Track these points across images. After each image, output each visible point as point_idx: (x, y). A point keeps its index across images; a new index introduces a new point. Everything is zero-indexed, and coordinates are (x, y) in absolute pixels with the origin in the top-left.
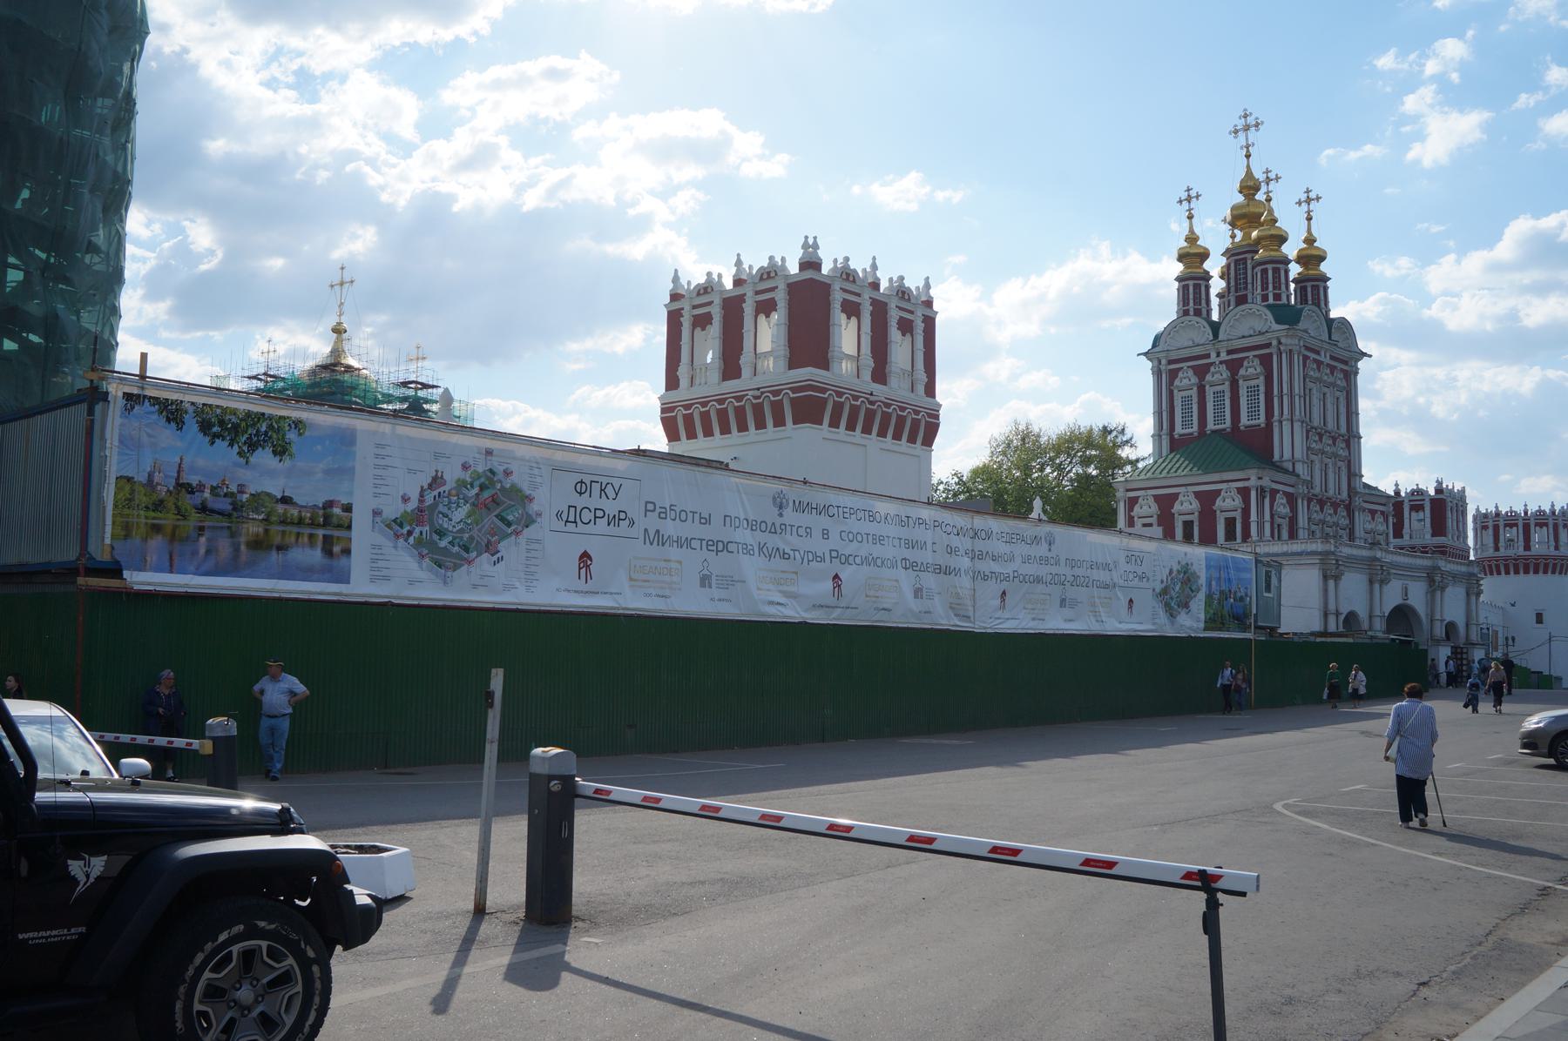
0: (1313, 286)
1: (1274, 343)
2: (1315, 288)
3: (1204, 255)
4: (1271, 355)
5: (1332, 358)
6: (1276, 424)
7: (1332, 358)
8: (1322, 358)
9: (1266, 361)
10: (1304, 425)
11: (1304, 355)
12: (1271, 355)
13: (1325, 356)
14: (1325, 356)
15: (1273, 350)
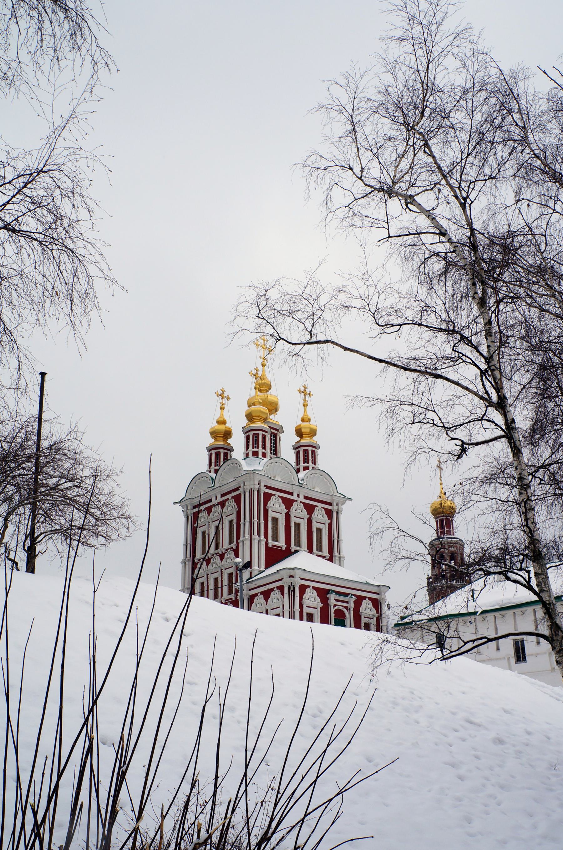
0: (304, 450)
1: (242, 485)
2: (306, 452)
3: (227, 434)
4: (240, 495)
5: (306, 498)
6: (241, 544)
7: (306, 498)
8: (295, 497)
9: (237, 499)
10: (263, 543)
11: (265, 493)
12: (240, 495)
13: (298, 496)
14: (298, 496)
15: (241, 489)
